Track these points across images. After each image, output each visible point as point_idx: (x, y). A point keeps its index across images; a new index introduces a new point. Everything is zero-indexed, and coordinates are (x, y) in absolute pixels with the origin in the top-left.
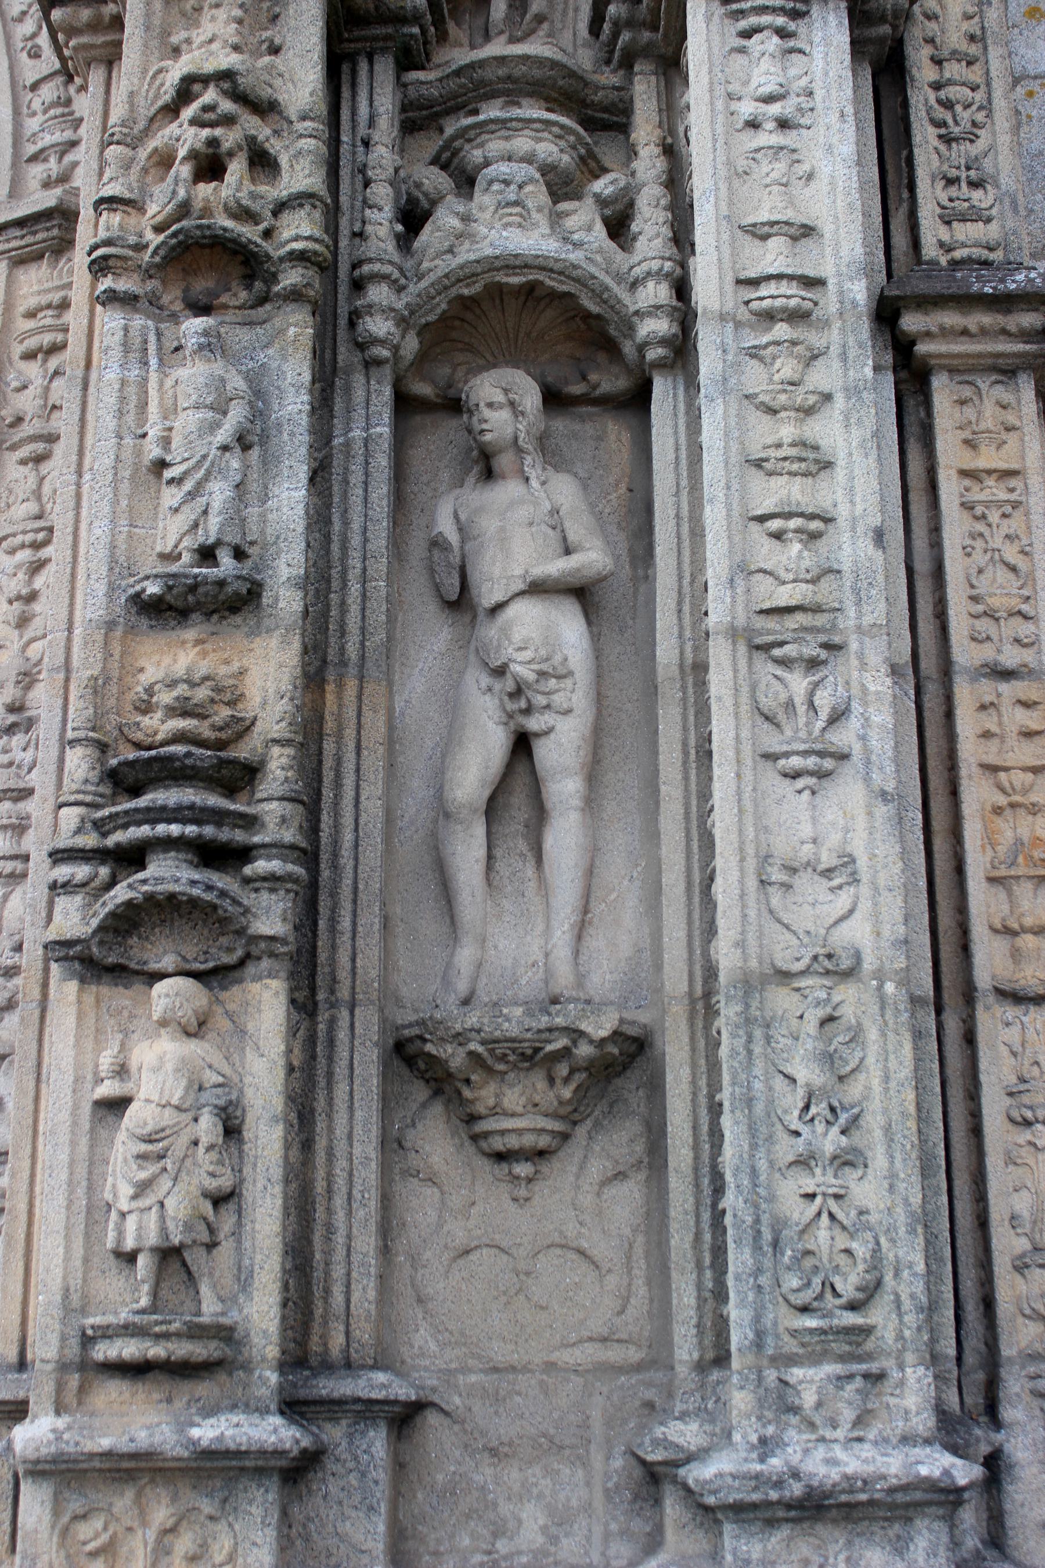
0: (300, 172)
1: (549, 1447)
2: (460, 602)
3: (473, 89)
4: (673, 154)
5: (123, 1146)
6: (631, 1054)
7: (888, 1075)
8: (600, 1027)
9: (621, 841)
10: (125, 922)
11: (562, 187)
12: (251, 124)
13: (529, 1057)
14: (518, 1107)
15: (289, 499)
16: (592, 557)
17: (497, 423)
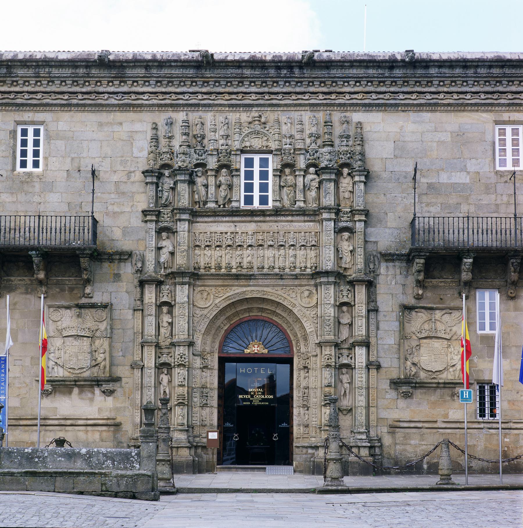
0: (333, 360)
1: (346, 430)
2: (342, 382)
3: (342, 349)
4: (355, 354)
5: (326, 415)
6: (351, 410)
7: (364, 412)
8: (350, 408)
9: (351, 397)
10: (326, 404)
11: (348, 356)
12: (331, 357)
13: (345, 410)
14: (345, 412)
15: (333, 380)
16: (349, 381)
17: (344, 372)
